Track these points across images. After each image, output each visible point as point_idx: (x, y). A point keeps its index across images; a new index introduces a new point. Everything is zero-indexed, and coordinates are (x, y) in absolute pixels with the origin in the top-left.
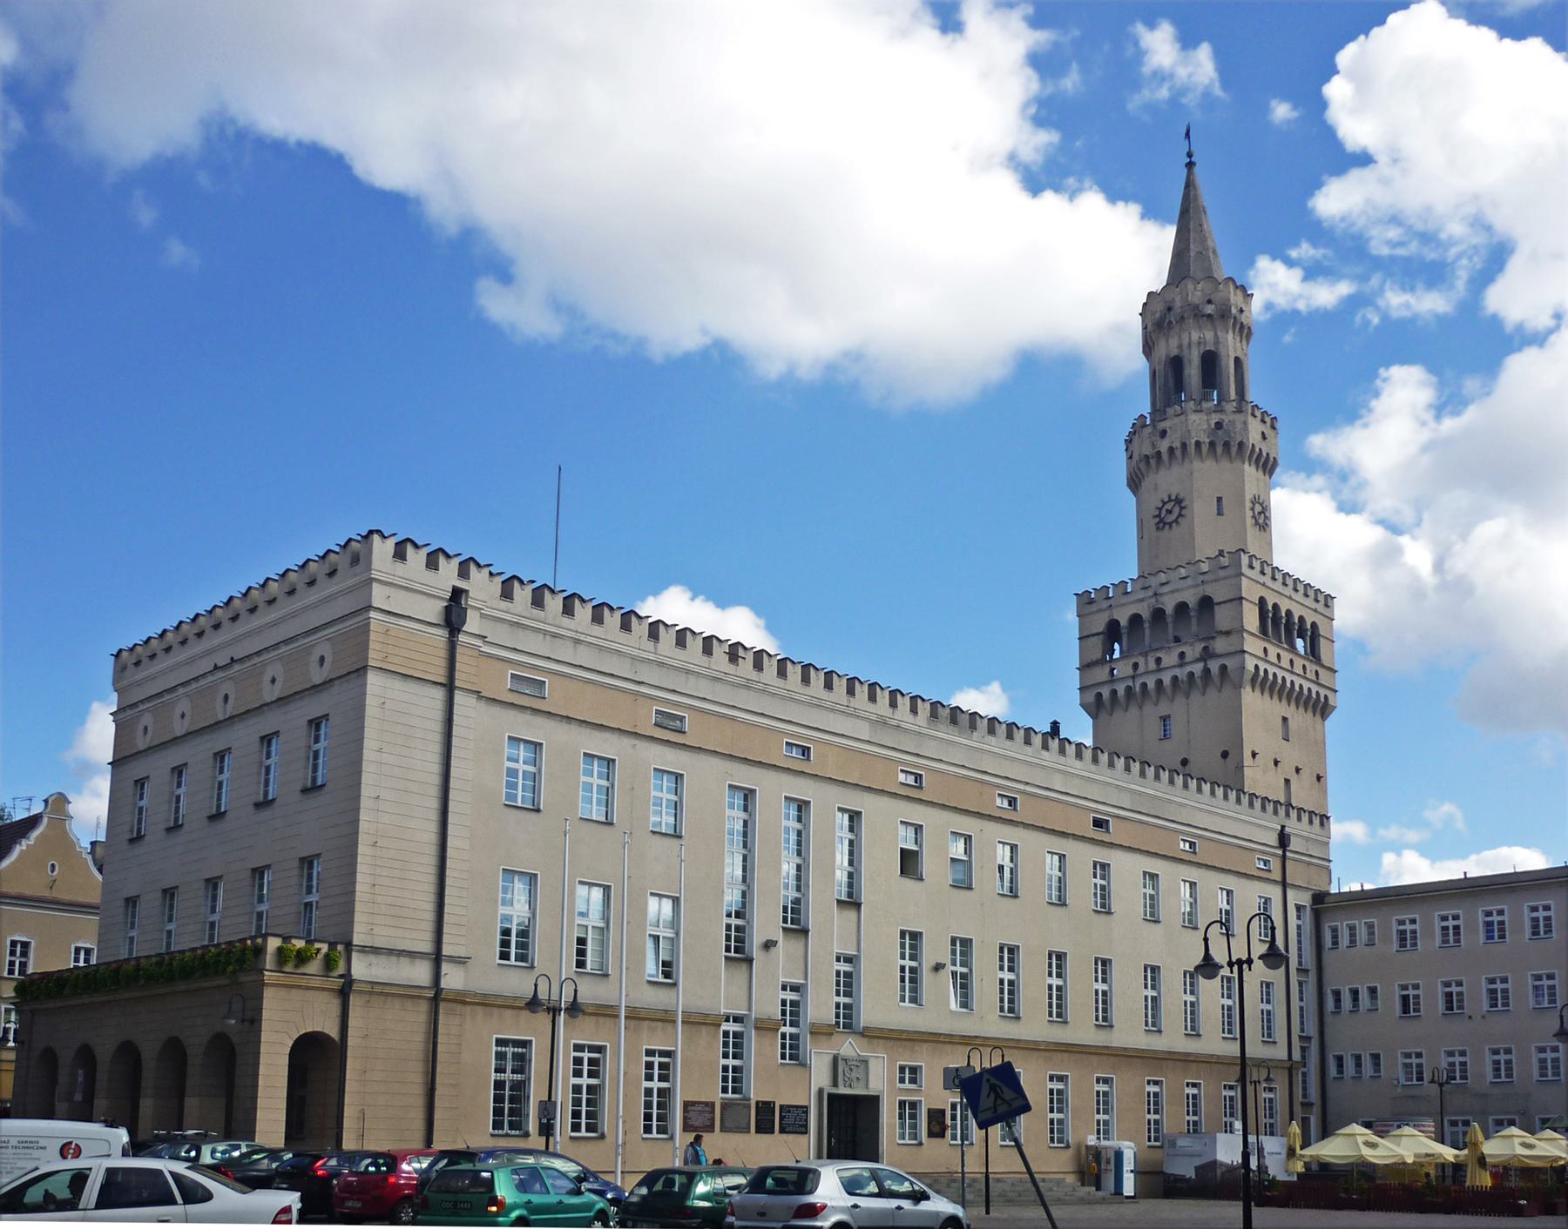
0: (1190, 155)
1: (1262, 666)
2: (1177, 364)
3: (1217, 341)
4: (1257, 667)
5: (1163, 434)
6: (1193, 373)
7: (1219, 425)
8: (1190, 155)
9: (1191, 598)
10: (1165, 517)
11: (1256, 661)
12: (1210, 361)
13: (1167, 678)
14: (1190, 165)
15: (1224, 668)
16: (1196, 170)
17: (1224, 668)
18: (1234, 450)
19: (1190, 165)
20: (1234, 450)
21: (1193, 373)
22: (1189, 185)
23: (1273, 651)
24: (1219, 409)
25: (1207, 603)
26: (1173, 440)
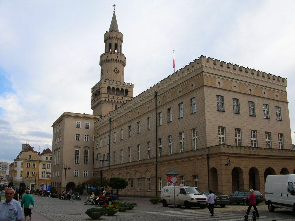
0: (114, 10)
2: (110, 45)
3: (117, 42)
5: (108, 56)
6: (113, 46)
8: (114, 10)
12: (116, 45)
14: (114, 11)
18: (120, 62)
19: (114, 11)
21: (113, 46)
22: (114, 15)
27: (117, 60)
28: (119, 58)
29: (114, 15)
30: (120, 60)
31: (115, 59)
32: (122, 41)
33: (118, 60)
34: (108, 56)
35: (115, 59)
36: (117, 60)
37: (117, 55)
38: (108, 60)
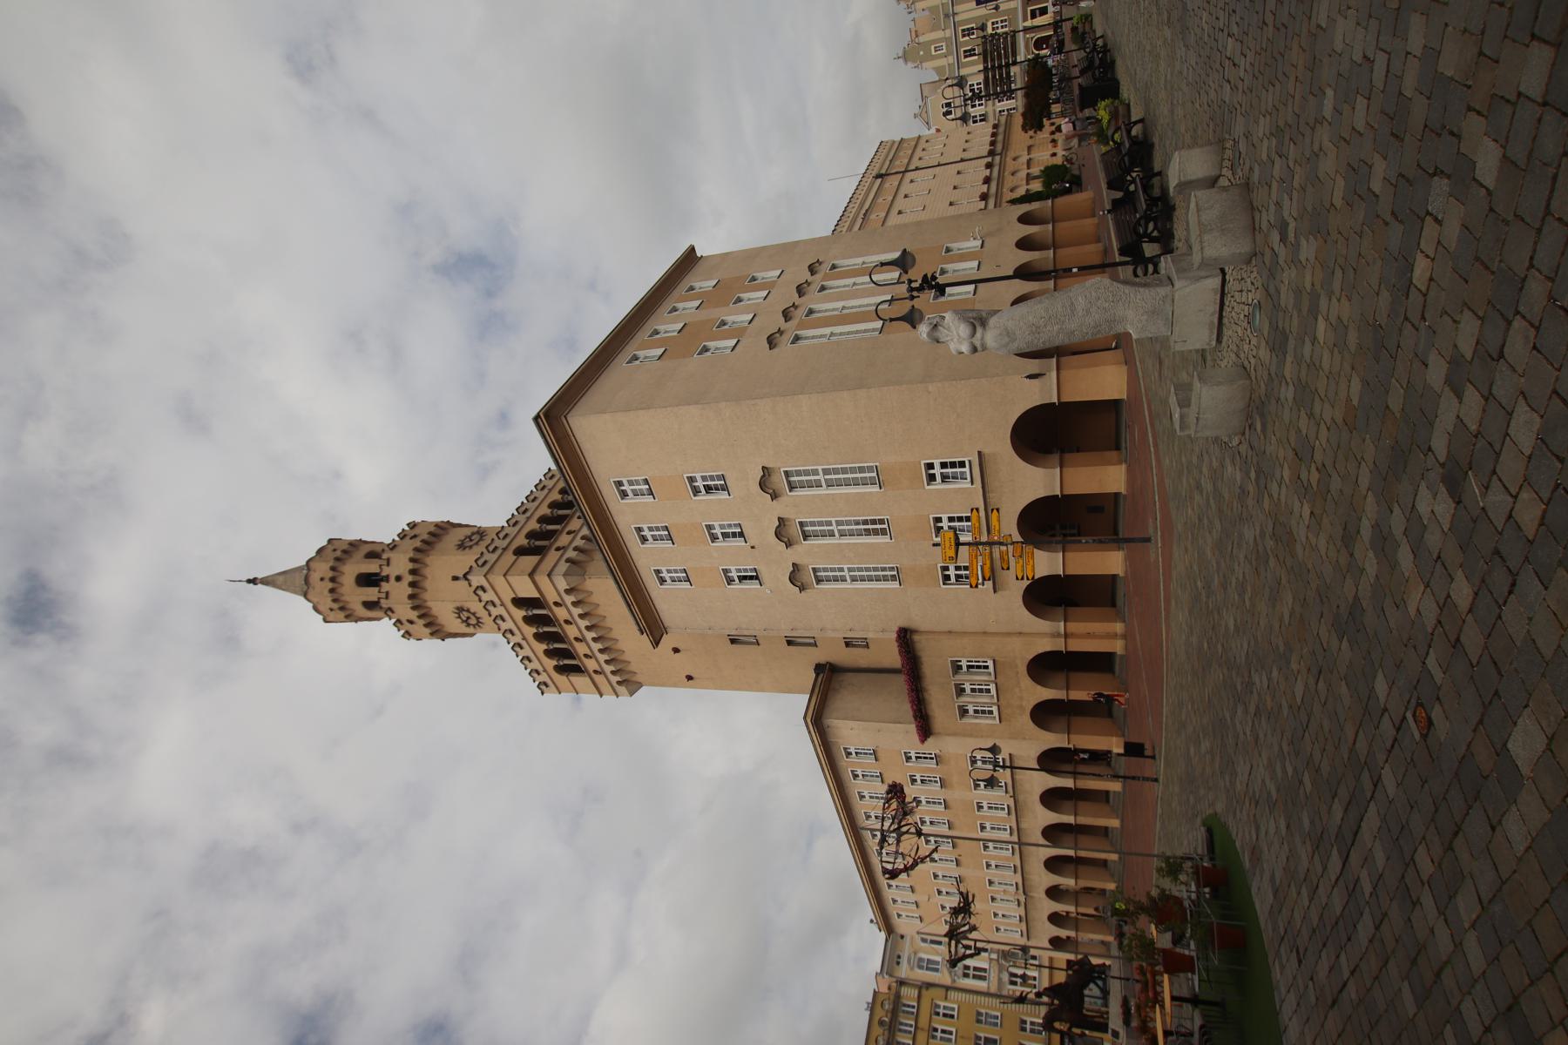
1: (571, 554)
2: (370, 605)
4: (568, 561)
5: (411, 622)
7: (398, 579)
8: (249, 581)
9: (519, 614)
10: (470, 622)
11: (563, 561)
12: (367, 580)
13: (590, 635)
14: (253, 581)
15: (568, 592)
16: (260, 576)
17: (568, 592)
19: (253, 581)
20: (417, 566)
21: (371, 593)
22: (266, 581)
23: (564, 540)
24: (387, 579)
25: (519, 602)
26: (413, 615)
27: (410, 578)
28: (400, 564)
29: (266, 581)
30: (411, 566)
31: (410, 591)
32: (355, 545)
33: (413, 572)
34: (411, 622)
35: (410, 591)
36: (410, 578)
37: (392, 579)
38: (422, 622)
